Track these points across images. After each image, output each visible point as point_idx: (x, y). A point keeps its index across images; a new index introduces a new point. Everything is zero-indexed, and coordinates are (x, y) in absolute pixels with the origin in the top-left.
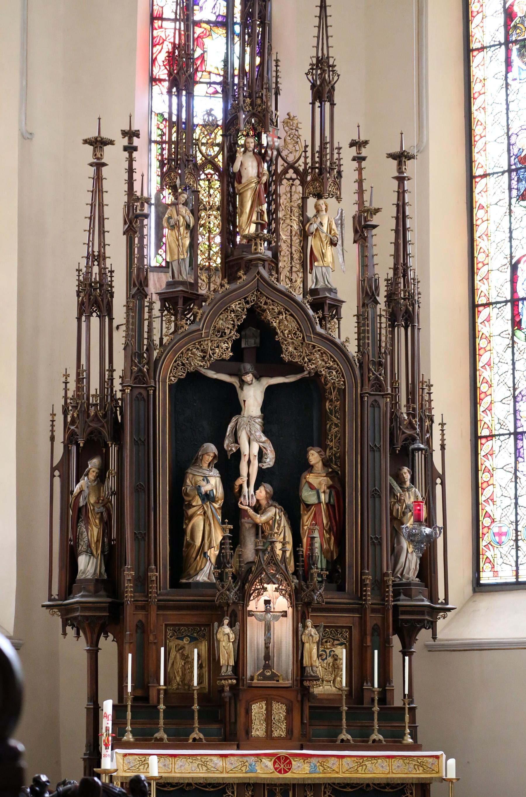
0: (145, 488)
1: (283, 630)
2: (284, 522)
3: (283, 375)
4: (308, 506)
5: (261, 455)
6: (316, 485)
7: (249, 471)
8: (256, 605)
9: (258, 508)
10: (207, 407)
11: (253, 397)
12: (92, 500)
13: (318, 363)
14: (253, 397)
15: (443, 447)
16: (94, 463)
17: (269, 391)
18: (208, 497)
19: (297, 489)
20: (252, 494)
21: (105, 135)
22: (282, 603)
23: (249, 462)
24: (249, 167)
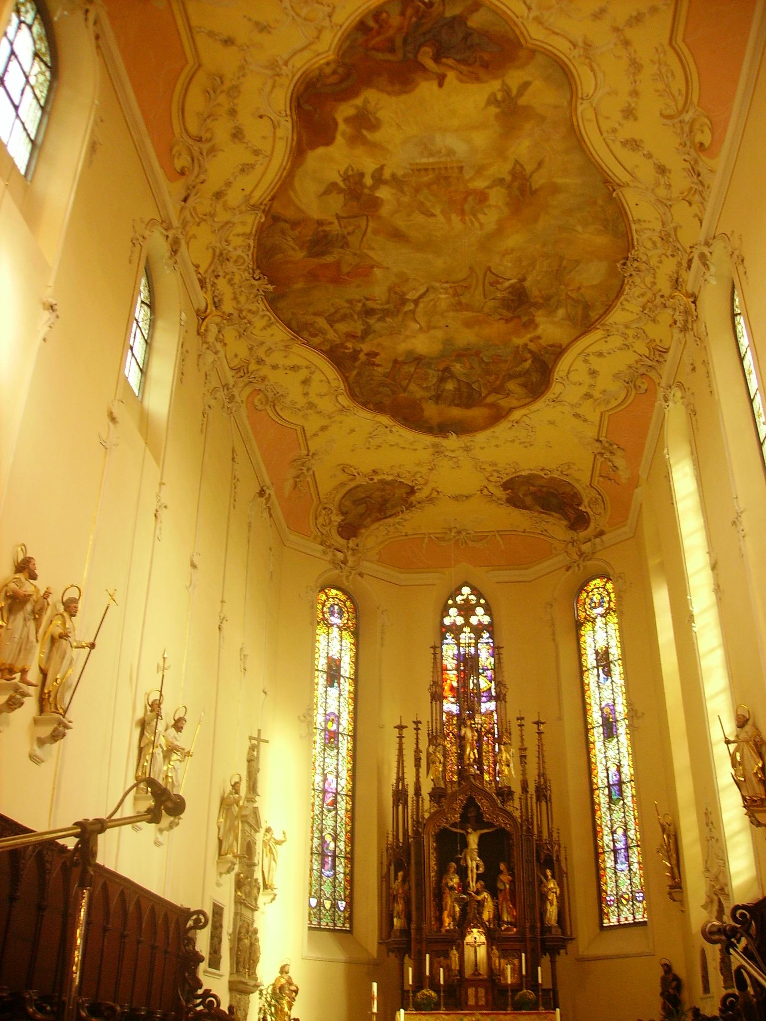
0: (420, 884)
1: (482, 952)
2: (489, 899)
3: (488, 828)
4: (501, 890)
5: (478, 867)
7: (472, 876)
8: (469, 939)
9: (478, 893)
10: (450, 846)
11: (473, 840)
12: (400, 891)
13: (501, 821)
14: (473, 840)
15: (566, 859)
16: (400, 874)
17: (482, 838)
18: (452, 888)
20: (473, 885)
21: (403, 724)
22: (483, 939)
23: (472, 871)
24: (468, 733)
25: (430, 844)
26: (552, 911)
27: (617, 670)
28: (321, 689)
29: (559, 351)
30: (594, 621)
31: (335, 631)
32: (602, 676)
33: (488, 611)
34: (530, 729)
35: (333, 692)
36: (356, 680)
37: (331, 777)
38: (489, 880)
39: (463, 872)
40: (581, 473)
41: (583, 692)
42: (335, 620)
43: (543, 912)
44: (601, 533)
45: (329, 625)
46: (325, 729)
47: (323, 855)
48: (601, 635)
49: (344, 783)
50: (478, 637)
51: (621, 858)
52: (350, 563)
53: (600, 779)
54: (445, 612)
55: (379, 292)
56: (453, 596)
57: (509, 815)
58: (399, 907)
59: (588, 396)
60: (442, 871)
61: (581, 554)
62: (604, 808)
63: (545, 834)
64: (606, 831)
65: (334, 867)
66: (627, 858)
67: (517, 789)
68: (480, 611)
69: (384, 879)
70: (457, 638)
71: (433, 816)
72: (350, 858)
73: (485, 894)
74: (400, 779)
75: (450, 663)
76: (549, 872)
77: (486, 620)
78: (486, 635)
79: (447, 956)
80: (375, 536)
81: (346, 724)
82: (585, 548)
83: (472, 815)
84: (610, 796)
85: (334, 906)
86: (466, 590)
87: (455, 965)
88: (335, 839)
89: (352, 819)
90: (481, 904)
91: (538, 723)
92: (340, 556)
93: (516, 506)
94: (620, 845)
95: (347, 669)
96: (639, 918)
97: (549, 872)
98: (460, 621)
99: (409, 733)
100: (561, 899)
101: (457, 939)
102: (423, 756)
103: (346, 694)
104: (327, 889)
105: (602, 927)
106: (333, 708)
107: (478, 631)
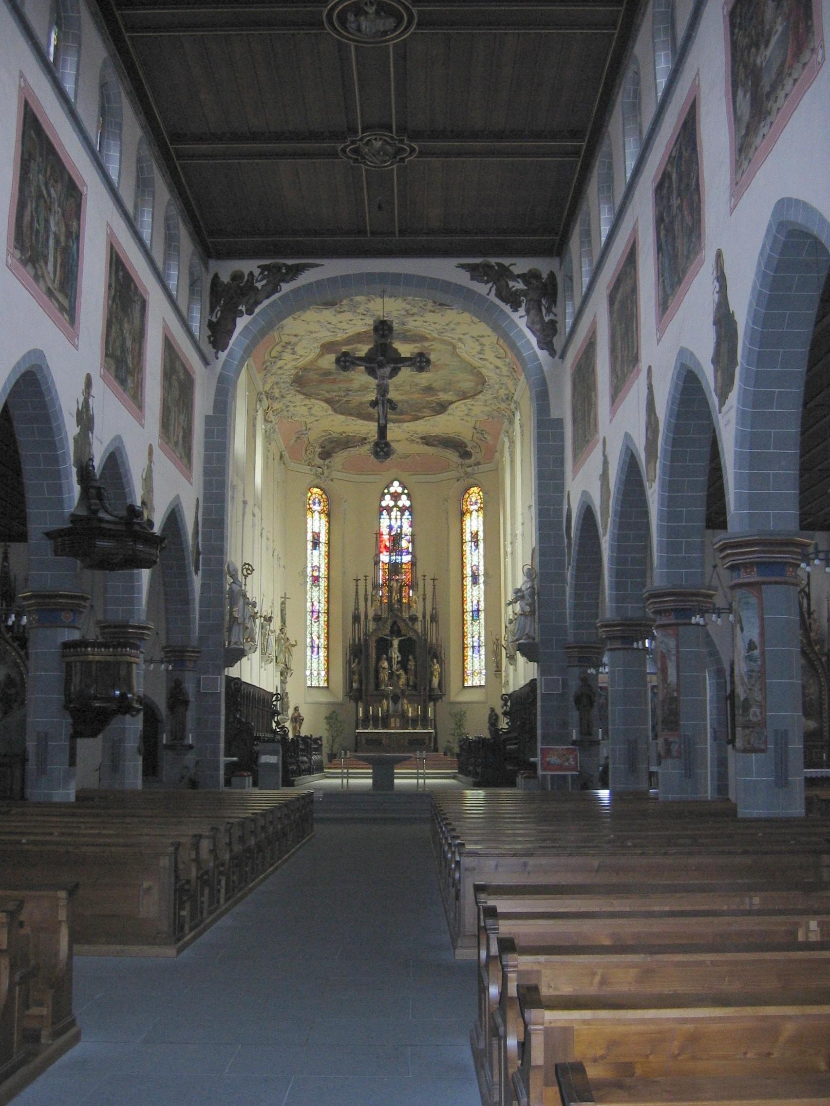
6: (411, 664)
7: (394, 662)
10: (383, 646)
11: (396, 643)
13: (411, 634)
14: (396, 643)
17: (400, 641)
18: (384, 668)
19: (407, 665)
20: (395, 667)
25: (373, 644)
26: (435, 681)
27: (481, 545)
28: (309, 552)
29: (452, 403)
30: (471, 513)
31: (316, 514)
32: (474, 548)
33: (409, 496)
34: (429, 583)
35: (316, 552)
36: (329, 544)
37: (316, 603)
38: (403, 664)
39: (389, 660)
40: (465, 433)
41: (462, 555)
42: (317, 508)
43: (431, 681)
44: (478, 464)
45: (313, 512)
46: (313, 576)
47: (312, 647)
48: (474, 523)
49: (323, 607)
50: (402, 514)
51: (476, 651)
52: (326, 474)
53: (468, 607)
54: (382, 497)
55: (355, 385)
56: (388, 487)
57: (415, 631)
58: (356, 677)
59: (467, 415)
60: (379, 659)
61: (466, 473)
62: (469, 622)
63: (434, 641)
64: (469, 636)
65: (318, 653)
66: (479, 651)
67: (420, 618)
68: (404, 497)
69: (348, 663)
70: (389, 514)
71: (375, 630)
72: (327, 648)
73: (401, 671)
74: (357, 609)
76: (435, 661)
77: (408, 504)
78: (407, 513)
79: (381, 702)
80: (340, 458)
81: (323, 572)
82: (469, 470)
83: (396, 631)
84: (473, 617)
85: (318, 674)
86: (396, 483)
87: (385, 708)
88: (319, 638)
89: (328, 626)
90: (399, 677)
91: (434, 580)
92: (320, 470)
93: (427, 445)
94: (476, 644)
95: (323, 538)
96: (483, 683)
97: (435, 661)
98: (392, 504)
99: (361, 584)
100: (441, 674)
102: (369, 597)
103: (323, 553)
104: (315, 665)
105: (464, 687)
106: (316, 563)
107: (402, 510)
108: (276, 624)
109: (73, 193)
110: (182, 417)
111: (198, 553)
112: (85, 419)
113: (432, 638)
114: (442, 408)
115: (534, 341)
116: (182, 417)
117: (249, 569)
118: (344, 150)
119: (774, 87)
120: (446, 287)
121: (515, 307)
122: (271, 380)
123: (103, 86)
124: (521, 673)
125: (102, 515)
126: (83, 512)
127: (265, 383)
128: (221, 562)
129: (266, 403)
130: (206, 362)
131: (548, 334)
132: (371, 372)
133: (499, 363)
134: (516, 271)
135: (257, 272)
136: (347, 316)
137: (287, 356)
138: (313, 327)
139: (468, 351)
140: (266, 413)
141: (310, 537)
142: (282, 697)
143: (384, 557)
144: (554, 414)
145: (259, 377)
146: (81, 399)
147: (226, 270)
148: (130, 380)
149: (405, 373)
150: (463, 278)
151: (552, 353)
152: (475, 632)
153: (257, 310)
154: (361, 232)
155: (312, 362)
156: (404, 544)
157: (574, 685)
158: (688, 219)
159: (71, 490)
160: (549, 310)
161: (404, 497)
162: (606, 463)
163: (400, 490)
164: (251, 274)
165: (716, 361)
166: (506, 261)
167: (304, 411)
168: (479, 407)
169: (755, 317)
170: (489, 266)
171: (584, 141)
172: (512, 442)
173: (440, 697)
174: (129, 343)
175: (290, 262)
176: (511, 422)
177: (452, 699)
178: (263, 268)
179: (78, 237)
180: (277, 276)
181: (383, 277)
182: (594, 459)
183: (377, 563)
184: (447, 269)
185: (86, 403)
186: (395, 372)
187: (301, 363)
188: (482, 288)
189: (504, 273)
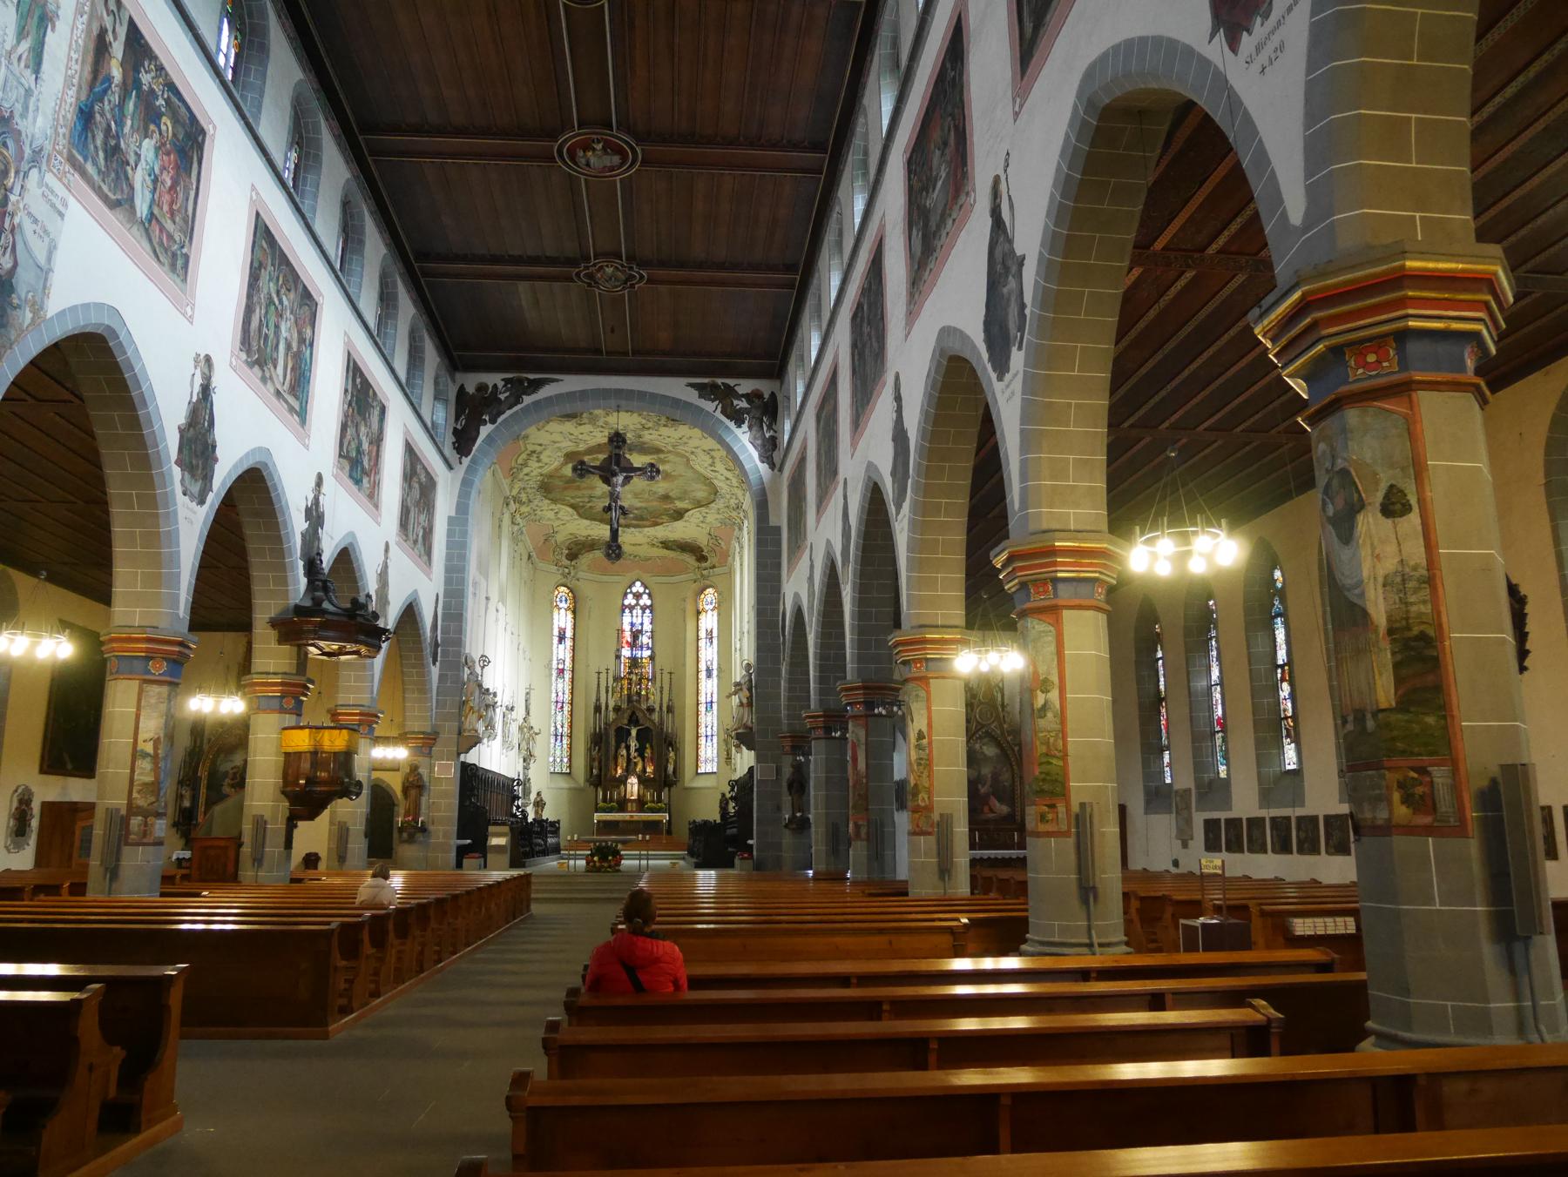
1: (636, 788)
6: (648, 753)
7: (633, 749)
10: (622, 735)
11: (634, 732)
14: (634, 732)
20: (633, 754)
25: (612, 733)
26: (671, 768)
27: (715, 641)
33: (650, 595)
34: (666, 677)
38: (640, 751)
39: (628, 748)
40: (703, 540)
42: (563, 605)
48: (709, 621)
49: (567, 697)
53: (702, 699)
68: (645, 597)
69: (589, 750)
74: (598, 699)
75: (627, 627)
77: (649, 603)
80: (586, 559)
81: (568, 665)
83: (634, 720)
86: (638, 584)
95: (569, 634)
98: (634, 602)
99: (603, 676)
101: (623, 781)
104: (558, 753)
107: (643, 609)
108: (519, 713)
109: (307, 300)
110: (422, 517)
111: (437, 645)
112: (315, 516)
113: (668, 727)
114: (679, 515)
115: (755, 455)
116: (422, 517)
117: (485, 661)
118: (578, 274)
119: (939, 227)
120: (676, 403)
121: (739, 423)
122: (518, 485)
123: (346, 205)
124: (745, 760)
125: (326, 605)
126: (308, 603)
127: (511, 488)
128: (459, 654)
129: (513, 506)
130: (450, 467)
131: (770, 449)
132: (607, 481)
133: (729, 475)
134: (741, 390)
135: (500, 384)
136: (587, 428)
137: (533, 464)
138: (557, 437)
139: (701, 463)
140: (513, 517)
141: (556, 632)
142: (525, 783)
143: (626, 652)
144: (773, 522)
145: (506, 482)
146: (311, 497)
147: (471, 381)
148: (365, 480)
149: (638, 483)
150: (692, 396)
151: (772, 466)
152: (709, 721)
153: (500, 420)
154: (598, 351)
155: (557, 470)
156: (645, 639)
157: (787, 772)
158: (875, 345)
159: (297, 582)
160: (770, 428)
161: (645, 597)
162: (812, 567)
163: (641, 590)
164: (495, 386)
165: (893, 474)
166: (731, 382)
167: (551, 515)
168: (712, 516)
169: (923, 433)
170: (714, 386)
171: (800, 275)
172: (742, 548)
173: (675, 783)
174: (365, 446)
175: (531, 376)
176: (741, 529)
177: (688, 784)
178: (506, 381)
179: (311, 345)
180: (520, 389)
181: (619, 393)
182: (804, 562)
183: (618, 657)
184: (677, 388)
185: (316, 499)
186: (627, 480)
187: (546, 470)
188: (709, 406)
189: (730, 392)
